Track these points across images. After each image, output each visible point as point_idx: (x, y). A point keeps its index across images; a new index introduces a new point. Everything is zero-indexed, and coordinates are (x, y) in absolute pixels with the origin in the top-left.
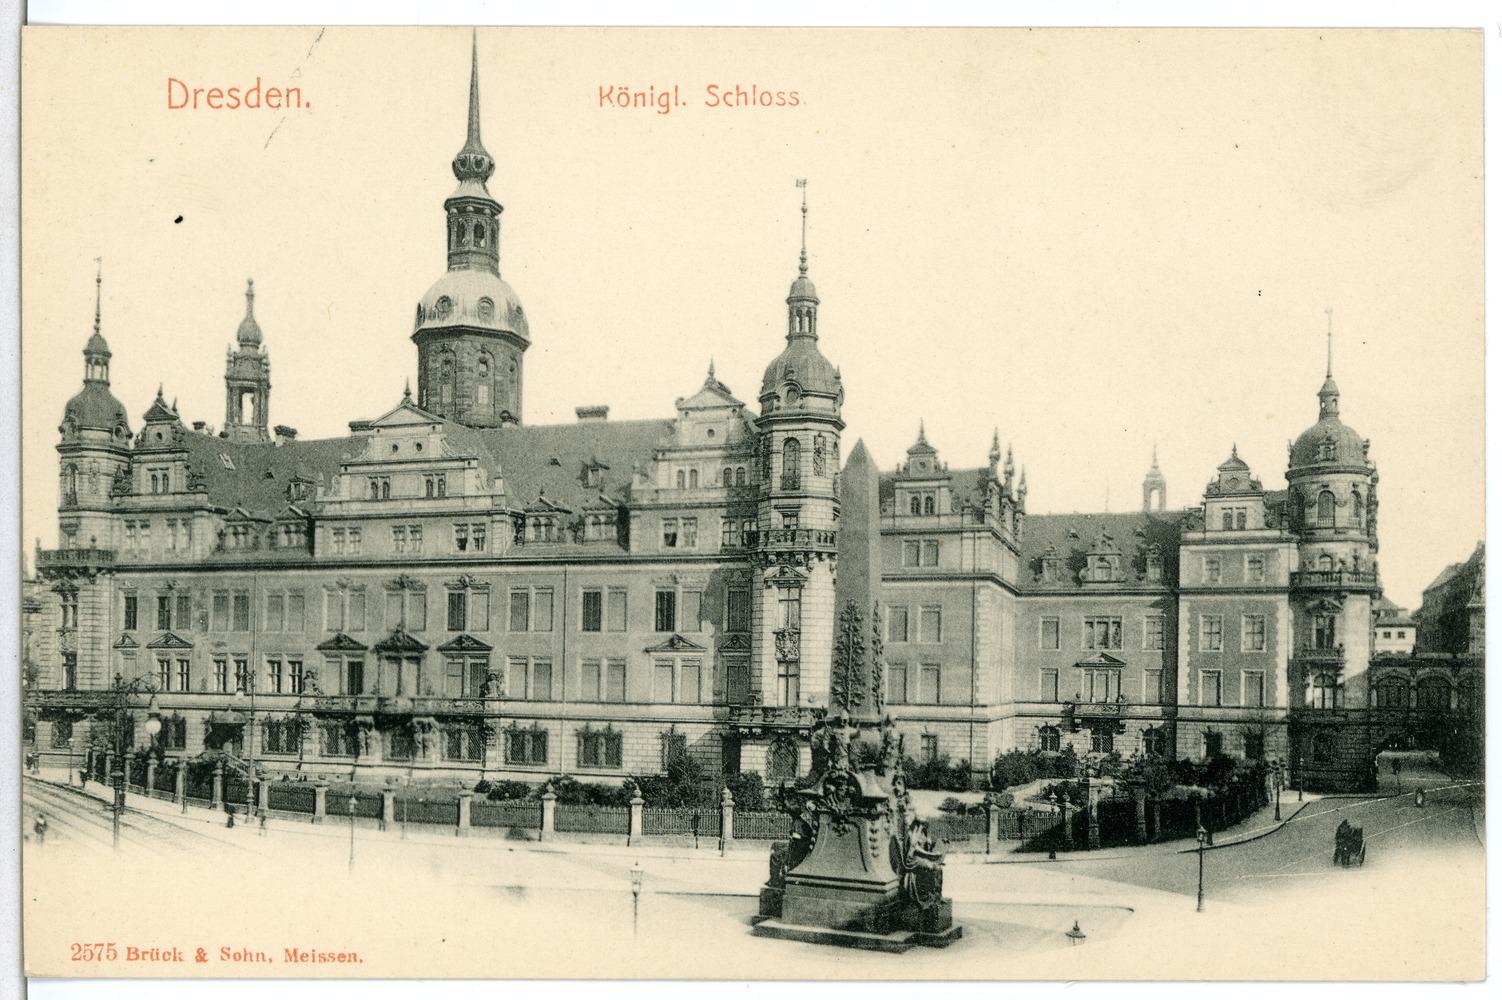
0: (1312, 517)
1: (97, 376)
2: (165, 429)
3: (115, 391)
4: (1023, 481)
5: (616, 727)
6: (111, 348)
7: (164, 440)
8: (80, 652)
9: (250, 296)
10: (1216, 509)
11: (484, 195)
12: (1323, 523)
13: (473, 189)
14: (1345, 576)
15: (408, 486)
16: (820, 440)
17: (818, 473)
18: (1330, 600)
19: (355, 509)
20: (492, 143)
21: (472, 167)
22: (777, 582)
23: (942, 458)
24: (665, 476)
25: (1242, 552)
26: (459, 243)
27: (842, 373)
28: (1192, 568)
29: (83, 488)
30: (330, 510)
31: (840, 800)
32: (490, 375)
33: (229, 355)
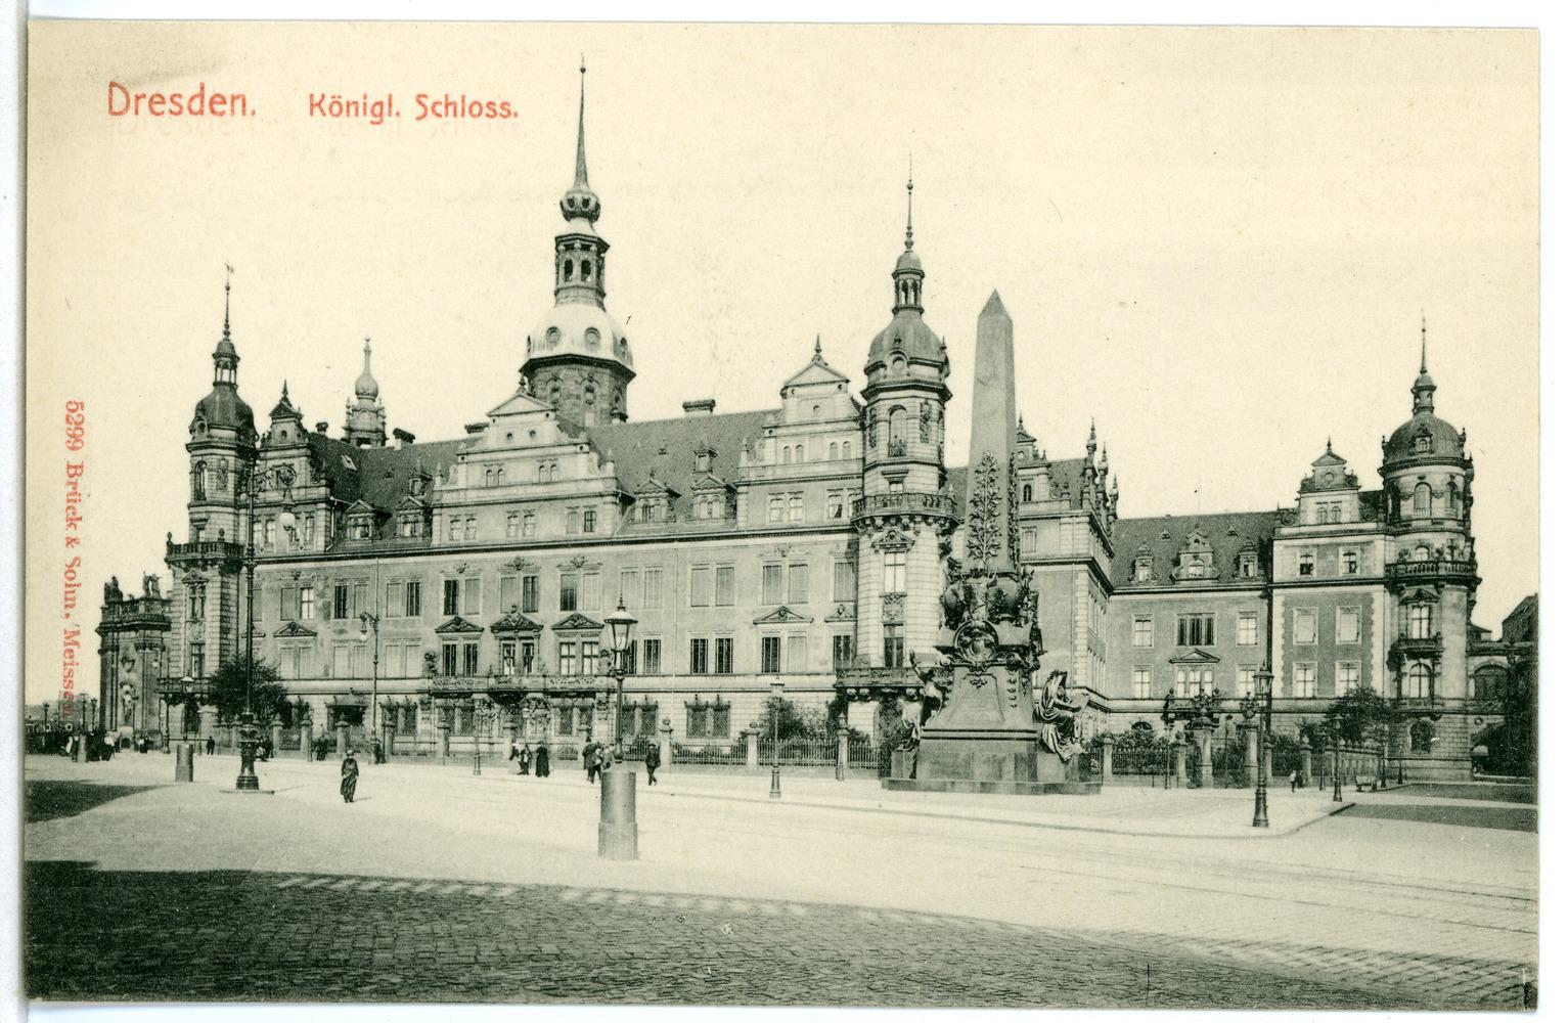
0: (1407, 509)
1: (226, 378)
2: (289, 427)
3: (245, 394)
4: (1115, 486)
5: (725, 698)
6: (239, 351)
7: (289, 437)
8: (208, 641)
9: (368, 352)
10: (1311, 502)
11: (590, 233)
12: (1420, 514)
13: (580, 226)
14: (1442, 565)
15: (521, 472)
16: (926, 407)
17: (925, 440)
18: (1429, 588)
19: (473, 496)
20: (599, 186)
21: (582, 209)
22: (883, 546)
23: (1040, 447)
24: (770, 451)
25: (1338, 545)
26: (566, 279)
27: (947, 344)
28: (1286, 561)
29: (209, 483)
30: (448, 499)
31: (976, 651)
32: (596, 402)
33: (348, 407)
